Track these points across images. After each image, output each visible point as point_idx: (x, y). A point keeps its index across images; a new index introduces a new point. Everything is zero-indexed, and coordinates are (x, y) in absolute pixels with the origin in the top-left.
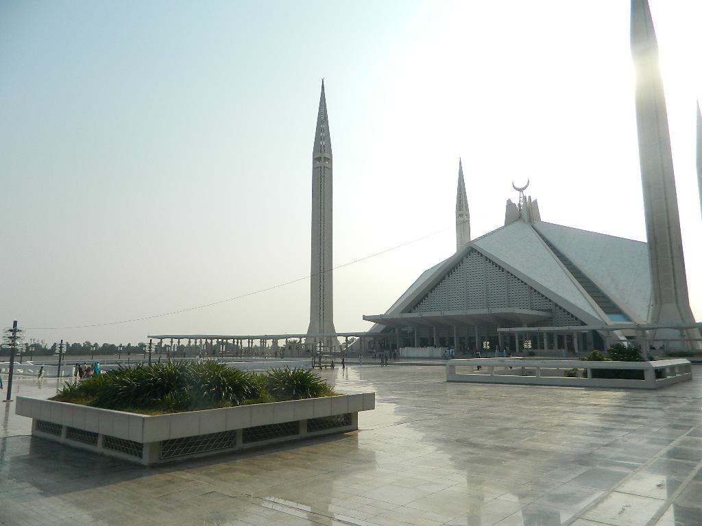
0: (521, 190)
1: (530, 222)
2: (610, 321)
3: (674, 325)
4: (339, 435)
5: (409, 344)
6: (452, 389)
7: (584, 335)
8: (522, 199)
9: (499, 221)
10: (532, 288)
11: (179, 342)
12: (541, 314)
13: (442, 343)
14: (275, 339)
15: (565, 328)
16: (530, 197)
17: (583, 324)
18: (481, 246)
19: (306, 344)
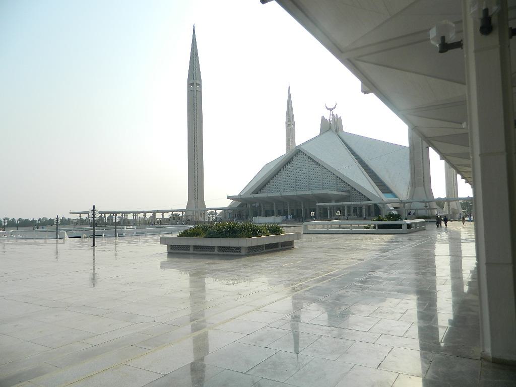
0: (331, 110)
1: (337, 132)
2: (385, 198)
3: (422, 200)
4: (290, 249)
5: (256, 215)
6: (305, 236)
7: (369, 207)
8: (331, 116)
9: (315, 131)
10: (338, 177)
11: (80, 216)
12: (344, 193)
13: (279, 214)
14: (163, 212)
15: (359, 203)
16: (337, 115)
17: (369, 200)
18: (305, 149)
19: (186, 216)
